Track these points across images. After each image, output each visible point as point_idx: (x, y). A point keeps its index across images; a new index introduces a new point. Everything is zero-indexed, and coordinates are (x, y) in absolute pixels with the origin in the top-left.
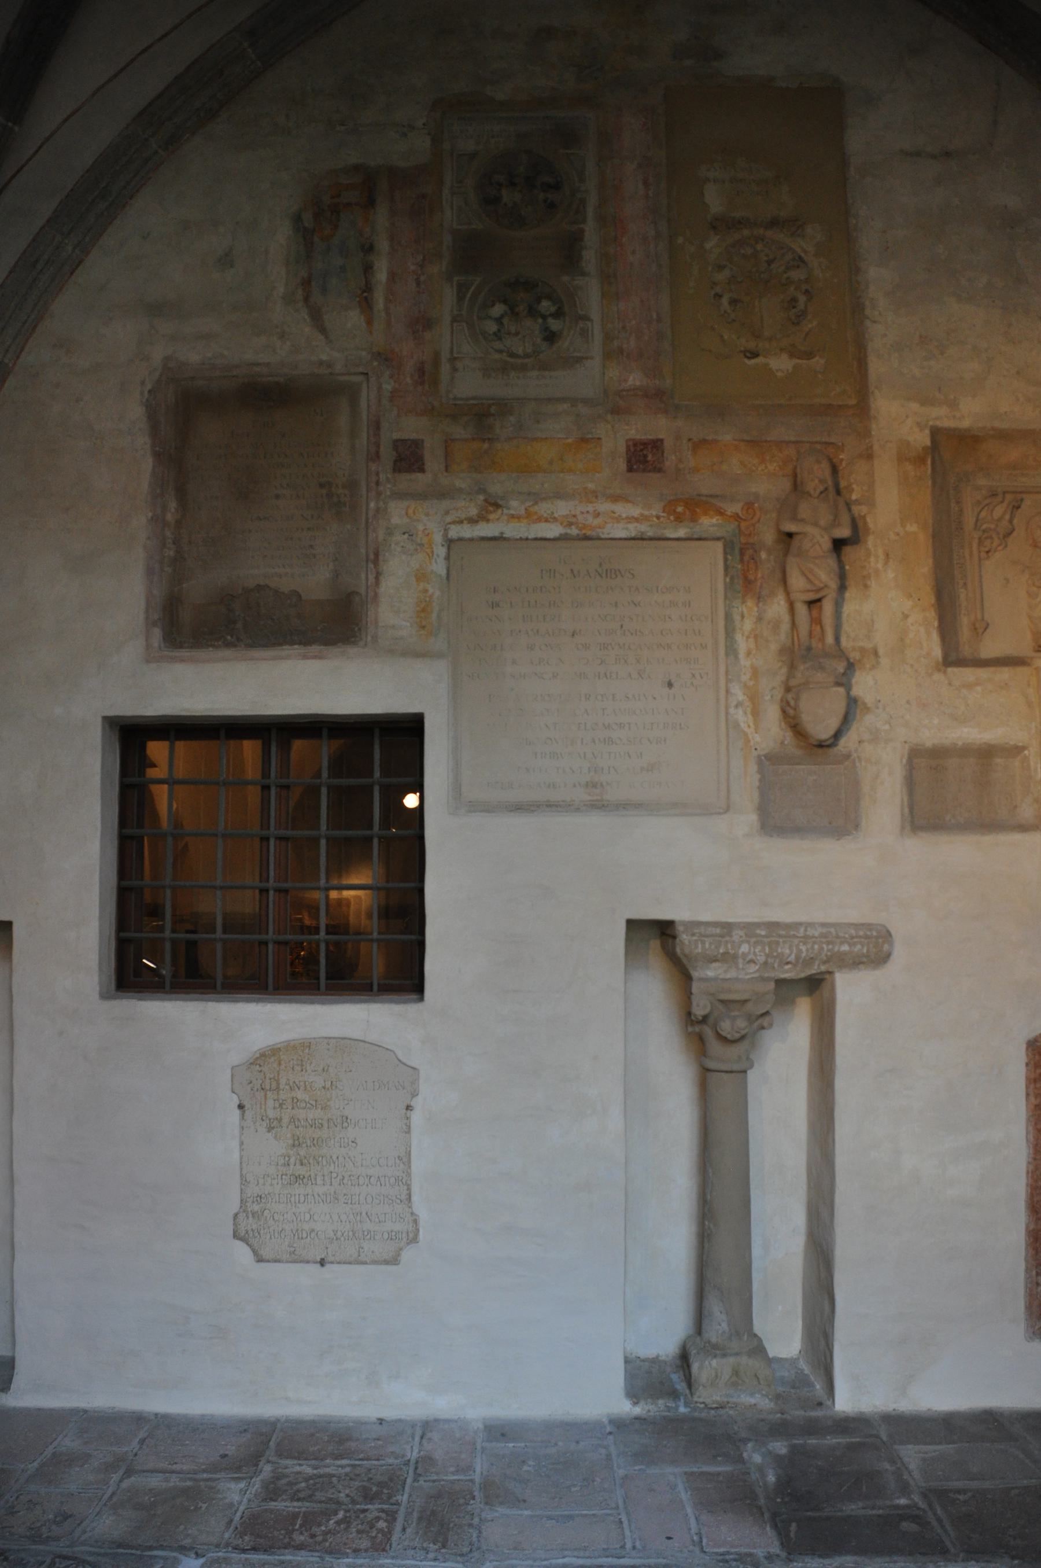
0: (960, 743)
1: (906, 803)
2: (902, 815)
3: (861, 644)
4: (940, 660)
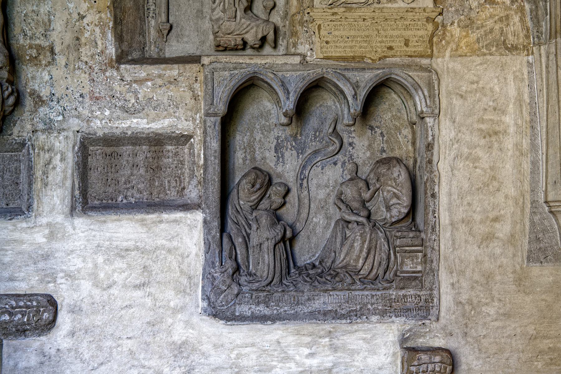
0: (129, 133)
1: (77, 186)
2: (73, 196)
3: (38, 42)
4: (114, 58)
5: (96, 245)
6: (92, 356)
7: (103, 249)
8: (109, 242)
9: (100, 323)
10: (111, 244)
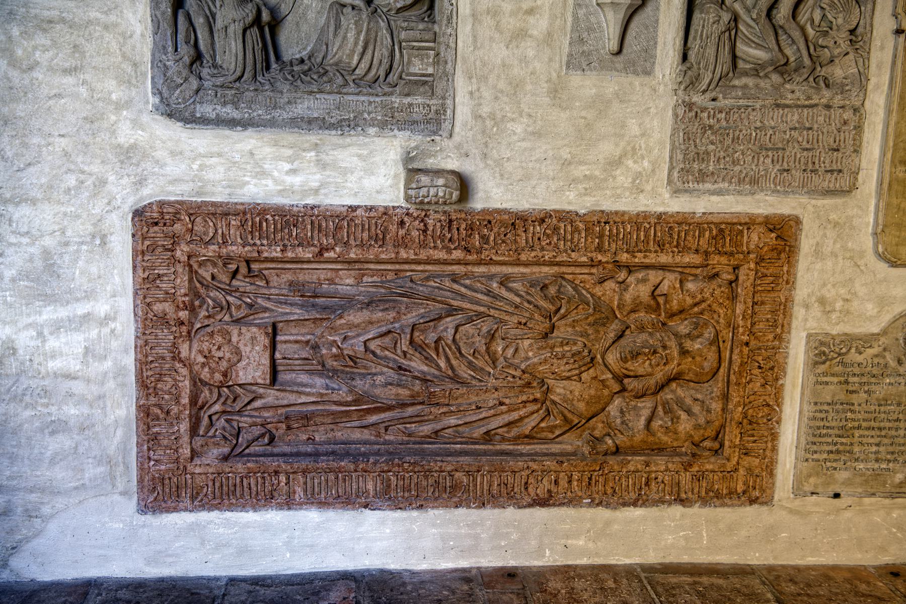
5: (8, 11)
6: (17, 155)
7: (18, 17)
8: (24, 10)
9: (23, 114)
10: (28, 12)
